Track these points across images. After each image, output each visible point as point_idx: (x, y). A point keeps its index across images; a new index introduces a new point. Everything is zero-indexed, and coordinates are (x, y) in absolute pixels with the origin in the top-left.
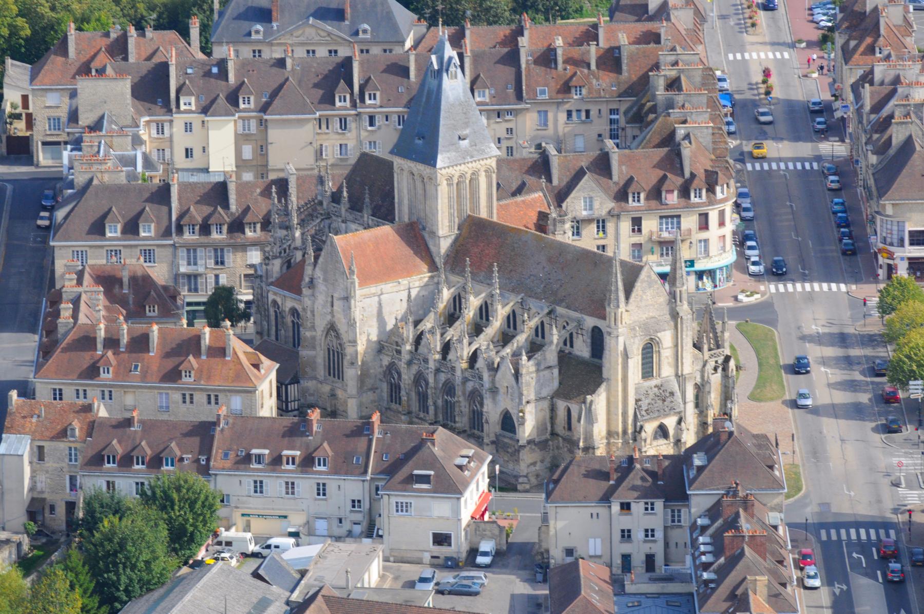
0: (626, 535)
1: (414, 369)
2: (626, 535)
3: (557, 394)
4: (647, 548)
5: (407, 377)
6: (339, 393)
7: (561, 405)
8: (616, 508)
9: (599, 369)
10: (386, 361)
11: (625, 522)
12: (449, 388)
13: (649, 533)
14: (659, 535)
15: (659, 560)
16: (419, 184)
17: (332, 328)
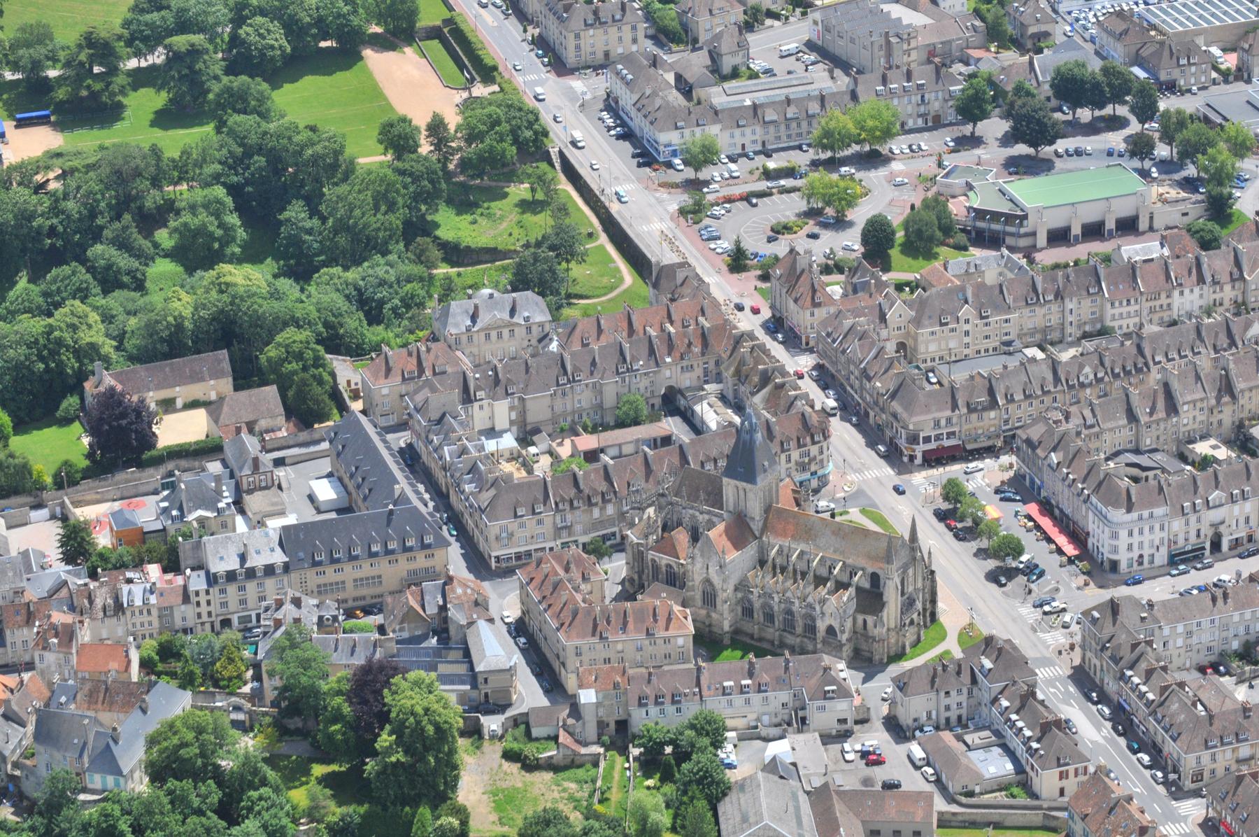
0: (948, 708)
1: (761, 600)
2: (948, 708)
3: (857, 611)
4: (958, 712)
5: (757, 605)
6: (713, 615)
7: (860, 618)
8: (942, 694)
9: (881, 595)
10: (740, 595)
11: (947, 701)
12: (789, 612)
13: (959, 704)
14: (964, 704)
15: (964, 718)
16: (742, 493)
17: (708, 581)
